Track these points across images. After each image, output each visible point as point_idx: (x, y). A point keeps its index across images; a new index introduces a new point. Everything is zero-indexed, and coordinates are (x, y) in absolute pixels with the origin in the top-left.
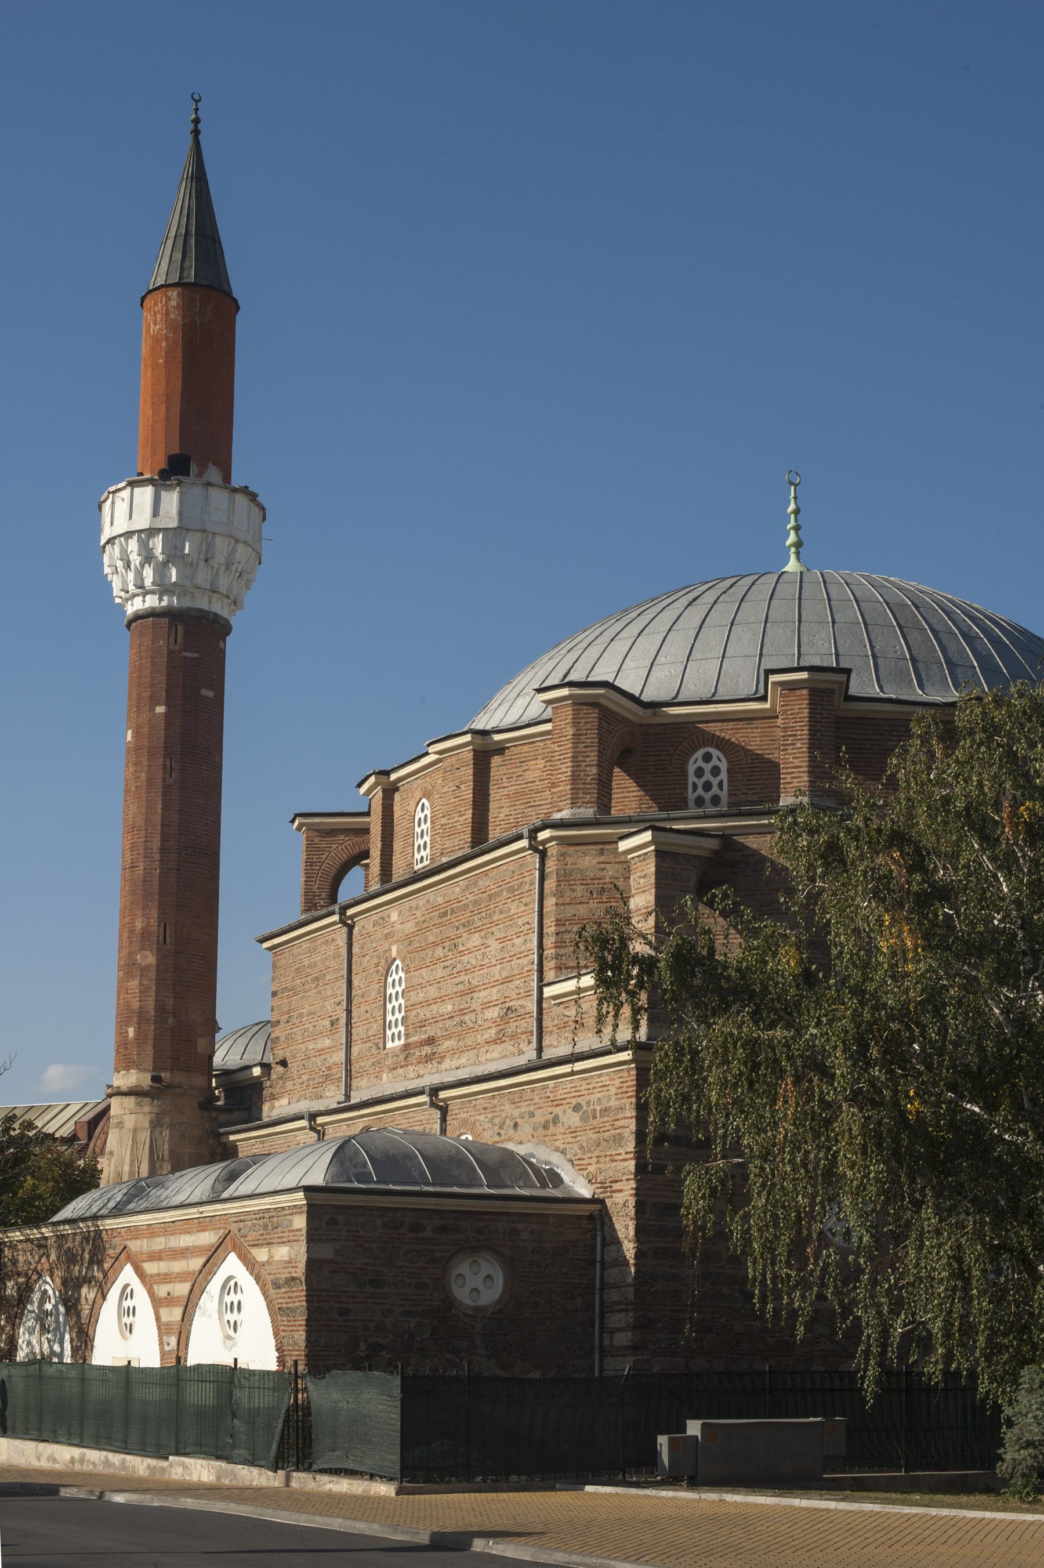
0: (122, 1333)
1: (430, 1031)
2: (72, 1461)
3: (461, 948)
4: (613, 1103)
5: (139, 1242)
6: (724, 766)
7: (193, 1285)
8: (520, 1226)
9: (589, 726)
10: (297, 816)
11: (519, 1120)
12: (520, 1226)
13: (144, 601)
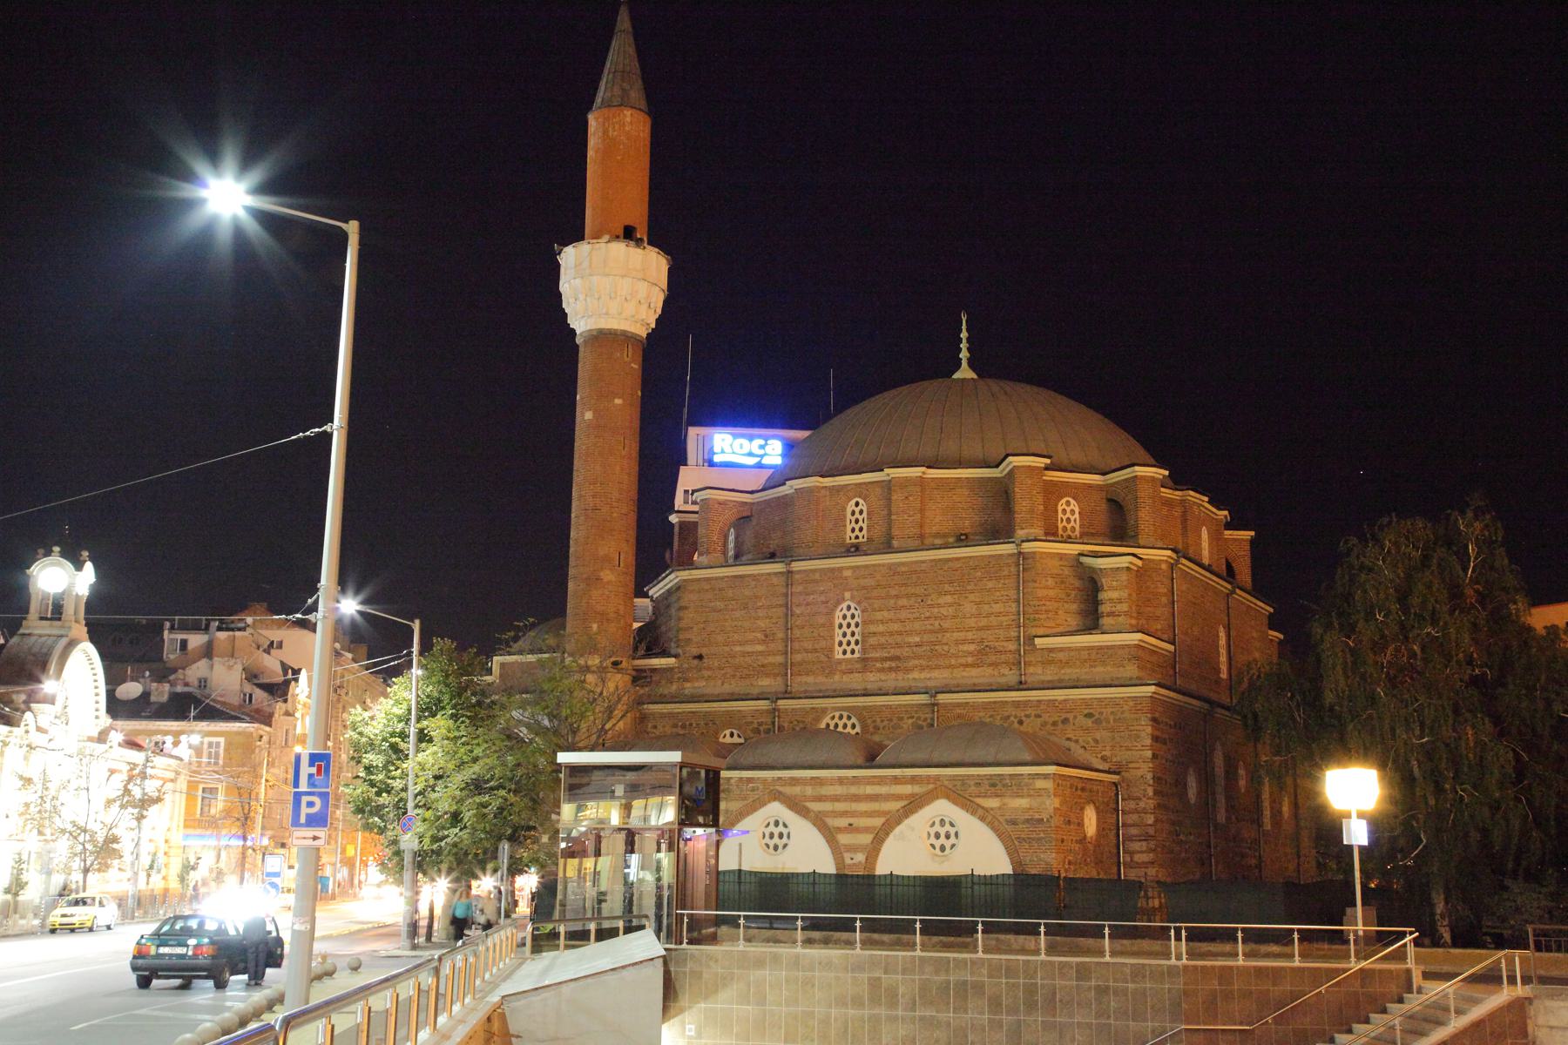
1: (897, 652)
4: (1127, 715)
6: (1077, 510)
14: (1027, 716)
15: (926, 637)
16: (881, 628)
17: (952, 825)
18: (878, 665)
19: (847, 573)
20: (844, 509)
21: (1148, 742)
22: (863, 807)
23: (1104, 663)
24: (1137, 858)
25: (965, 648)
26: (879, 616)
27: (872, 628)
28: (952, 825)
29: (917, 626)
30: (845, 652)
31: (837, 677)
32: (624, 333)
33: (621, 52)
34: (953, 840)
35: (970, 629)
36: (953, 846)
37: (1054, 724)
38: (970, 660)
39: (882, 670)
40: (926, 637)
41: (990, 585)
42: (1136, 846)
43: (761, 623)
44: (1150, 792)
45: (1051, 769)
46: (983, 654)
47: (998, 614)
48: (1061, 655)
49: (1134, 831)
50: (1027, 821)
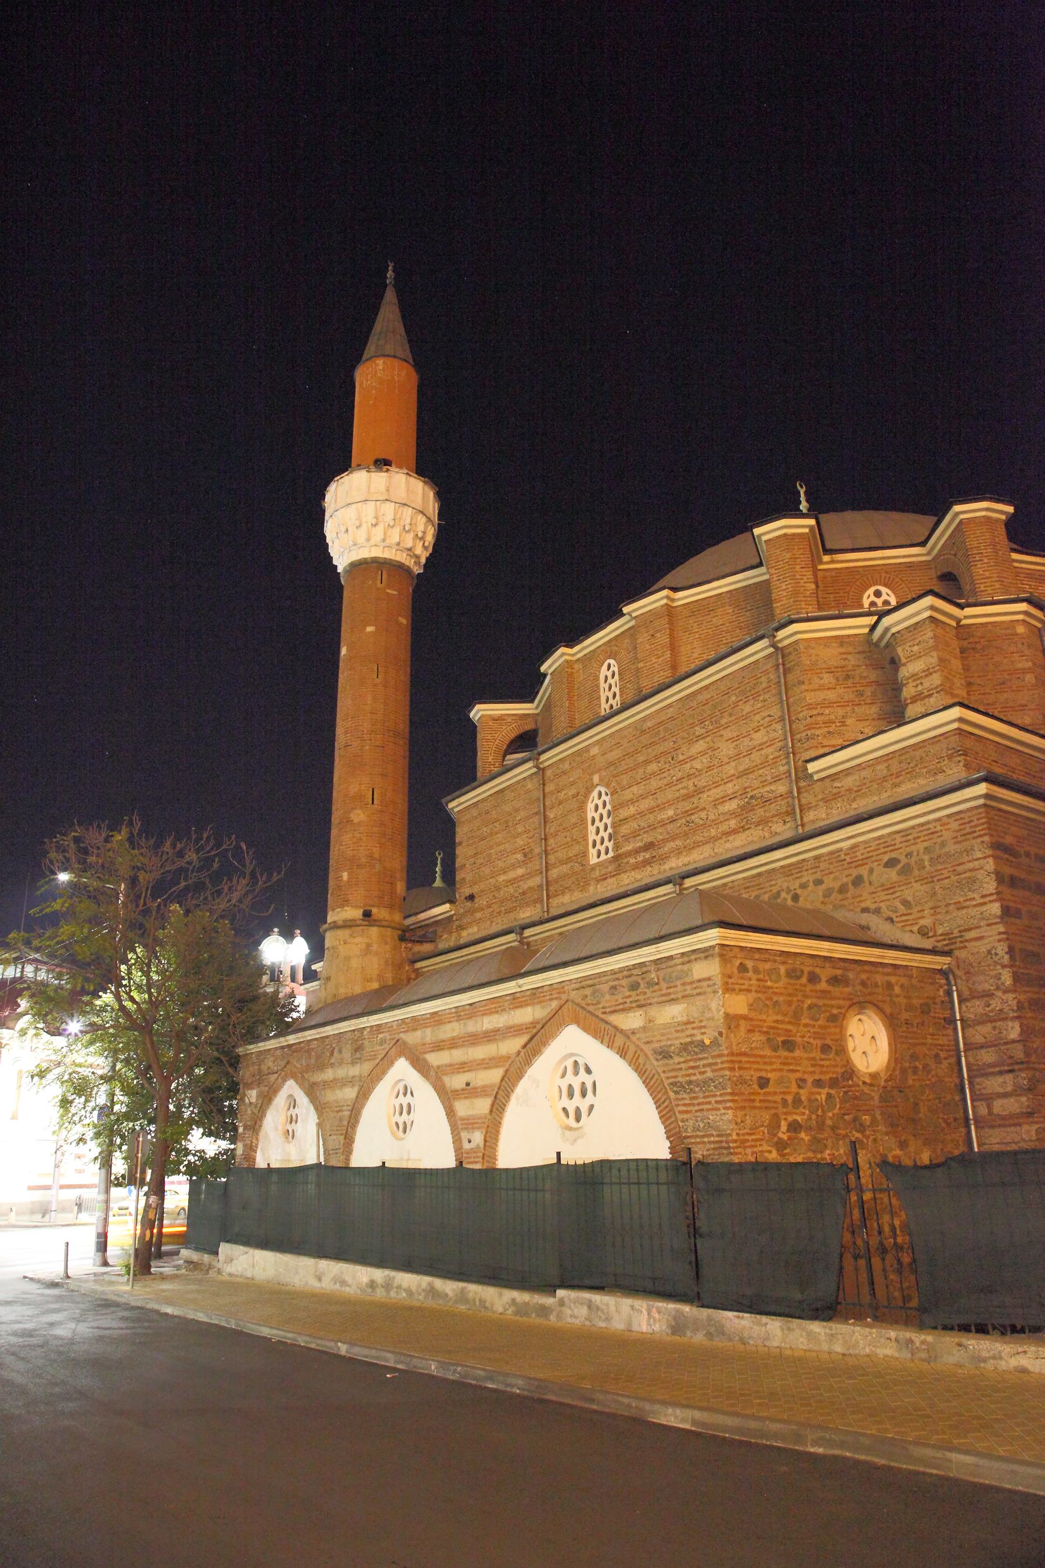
0: (392, 1133)
1: (647, 838)
2: (372, 1284)
3: (681, 757)
4: (951, 848)
5: (419, 1033)
7: (507, 1071)
8: (893, 979)
9: (801, 551)
11: (799, 891)
12: (893, 979)
14: (803, 886)
16: (632, 810)
17: (588, 1071)
18: (632, 861)
19: (595, 751)
20: (597, 678)
21: (991, 886)
22: (480, 1052)
23: (912, 774)
24: (1000, 1106)
26: (628, 794)
27: (624, 813)
28: (588, 1071)
29: (670, 794)
30: (599, 856)
31: (592, 889)
32: (375, 560)
33: (389, 314)
35: (731, 779)
36: (592, 1107)
37: (843, 889)
38: (733, 823)
41: (747, 708)
42: (994, 1084)
43: (520, 842)
44: (1007, 978)
45: (712, 936)
47: (760, 747)
48: (849, 782)
49: (988, 1057)
50: (685, 1047)
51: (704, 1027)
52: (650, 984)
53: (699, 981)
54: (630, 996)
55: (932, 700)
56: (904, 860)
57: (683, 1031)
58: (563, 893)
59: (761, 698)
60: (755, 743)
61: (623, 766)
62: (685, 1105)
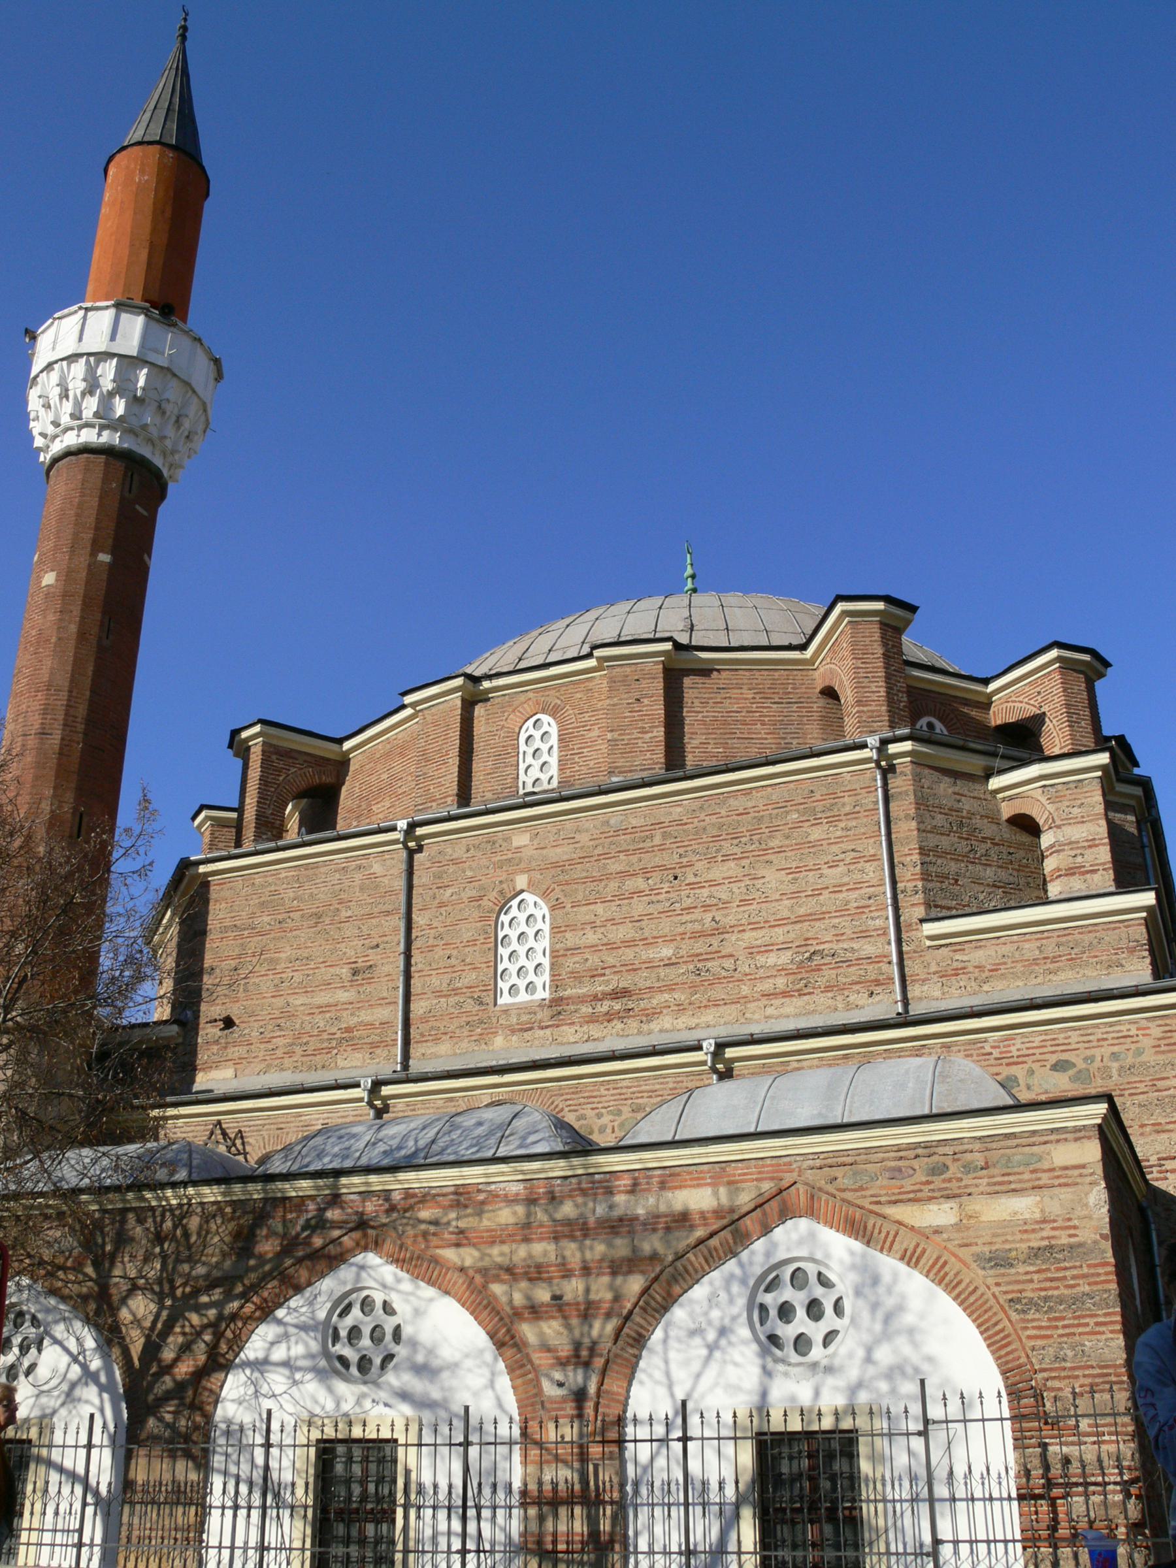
4: (1149, 1057)
10: (261, 721)
13: (78, 436)
15: (686, 947)
16: (591, 937)
18: (586, 1009)
25: (772, 959)
27: (571, 939)
29: (666, 926)
31: (499, 1041)
34: (830, 1320)
38: (781, 982)
39: (592, 1019)
40: (686, 947)
41: (816, 834)
46: (809, 965)
47: (837, 889)
51: (1075, 1227)
52: (968, 1168)
53: (1066, 1168)
54: (928, 1183)
55: (1097, 877)
56: (1081, 1065)
57: (1033, 1231)
58: (437, 1040)
59: (842, 825)
60: (826, 882)
61: (578, 872)
62: (1040, 1328)
